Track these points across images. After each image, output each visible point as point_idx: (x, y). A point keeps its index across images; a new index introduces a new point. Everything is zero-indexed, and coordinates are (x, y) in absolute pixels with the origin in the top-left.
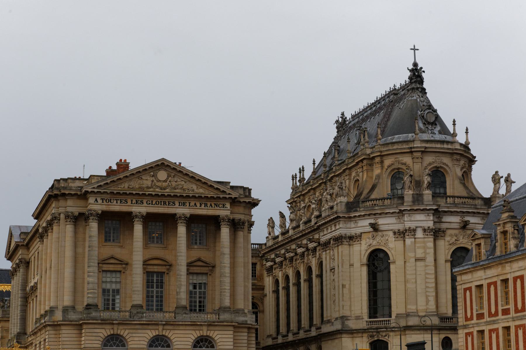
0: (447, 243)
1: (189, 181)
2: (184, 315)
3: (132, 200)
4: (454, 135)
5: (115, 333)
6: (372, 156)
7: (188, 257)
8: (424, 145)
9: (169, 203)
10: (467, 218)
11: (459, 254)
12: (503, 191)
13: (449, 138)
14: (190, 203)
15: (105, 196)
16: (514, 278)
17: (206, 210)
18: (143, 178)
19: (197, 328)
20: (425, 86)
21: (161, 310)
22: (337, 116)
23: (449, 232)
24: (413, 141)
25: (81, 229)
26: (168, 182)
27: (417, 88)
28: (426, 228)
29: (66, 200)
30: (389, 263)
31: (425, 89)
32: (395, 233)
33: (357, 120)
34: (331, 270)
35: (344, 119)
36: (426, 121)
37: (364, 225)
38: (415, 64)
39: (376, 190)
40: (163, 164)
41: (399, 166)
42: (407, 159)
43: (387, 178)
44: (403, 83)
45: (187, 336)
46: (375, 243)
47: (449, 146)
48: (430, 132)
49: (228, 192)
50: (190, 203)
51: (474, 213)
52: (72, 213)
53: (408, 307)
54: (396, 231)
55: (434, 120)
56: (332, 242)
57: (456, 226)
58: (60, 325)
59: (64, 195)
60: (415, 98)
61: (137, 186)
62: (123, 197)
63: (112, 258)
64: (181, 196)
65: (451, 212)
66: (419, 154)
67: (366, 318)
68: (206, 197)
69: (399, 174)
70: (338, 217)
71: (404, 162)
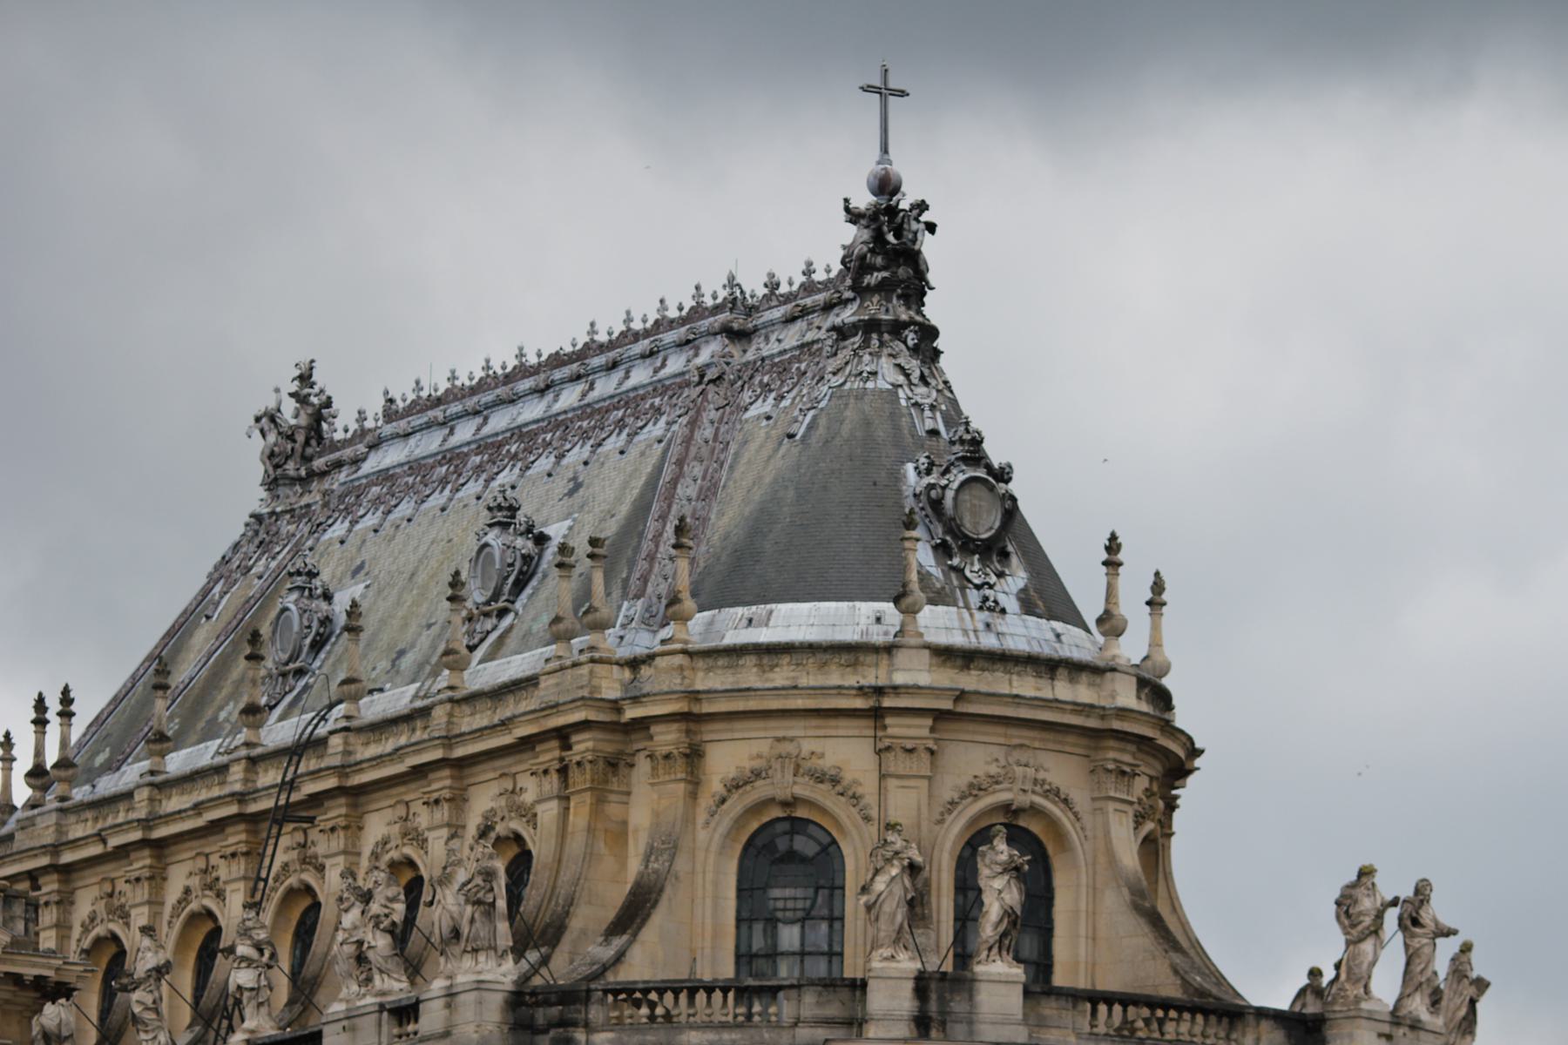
4: (1110, 624)
6: (631, 713)
8: (948, 678)
12: (1385, 985)
13: (1078, 644)
20: (934, 309)
22: (271, 387)
24: (889, 649)
27: (897, 328)
33: (431, 443)
35: (319, 414)
36: (952, 527)
38: (886, 186)
39: (658, 919)
41: (799, 791)
42: (848, 752)
43: (723, 850)
44: (791, 276)
47: (1083, 693)
55: (983, 528)
60: (882, 384)
66: (919, 729)
69: (792, 833)
71: (827, 763)
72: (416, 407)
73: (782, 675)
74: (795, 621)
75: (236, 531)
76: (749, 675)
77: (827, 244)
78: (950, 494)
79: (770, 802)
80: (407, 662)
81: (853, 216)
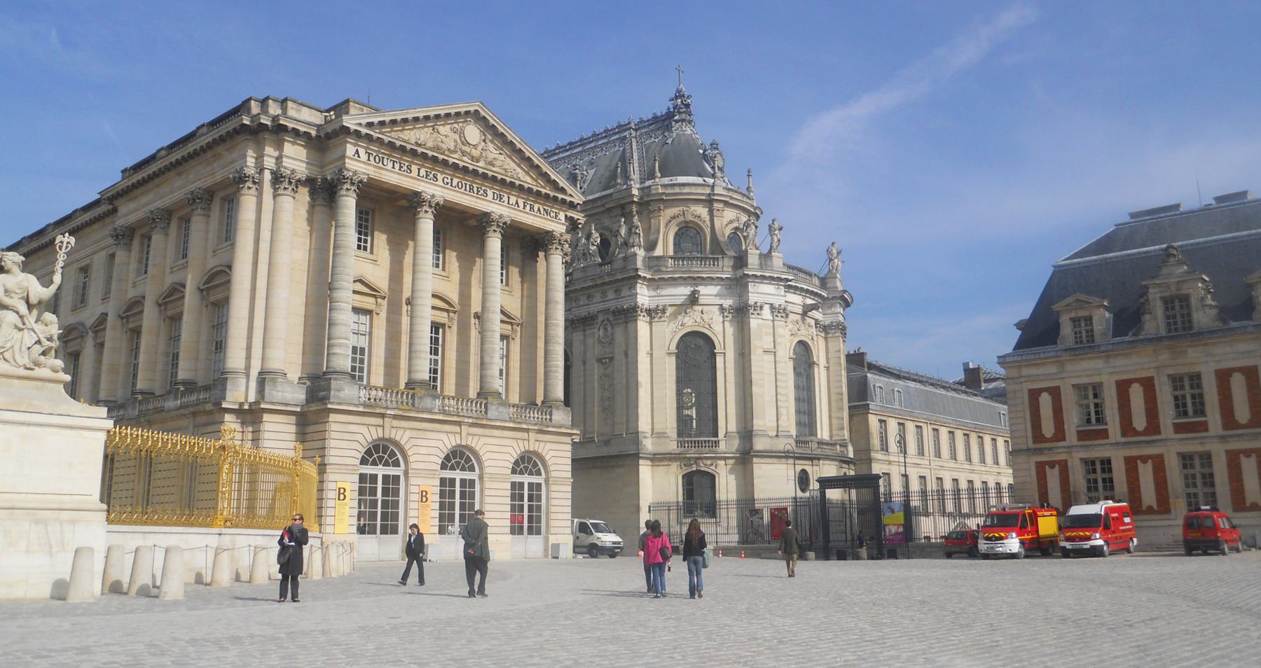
2: (501, 409)
5: (387, 436)
16: (1217, 372)
18: (441, 129)
19: (519, 435)
26: (480, 148)
34: (599, 360)
42: (702, 211)
45: (504, 450)
49: (569, 192)
53: (755, 421)
56: (601, 318)
61: (430, 144)
63: (360, 281)
64: (503, 182)
66: (720, 206)
67: (673, 433)
68: (538, 193)
73: (687, 190)
77: (661, 107)
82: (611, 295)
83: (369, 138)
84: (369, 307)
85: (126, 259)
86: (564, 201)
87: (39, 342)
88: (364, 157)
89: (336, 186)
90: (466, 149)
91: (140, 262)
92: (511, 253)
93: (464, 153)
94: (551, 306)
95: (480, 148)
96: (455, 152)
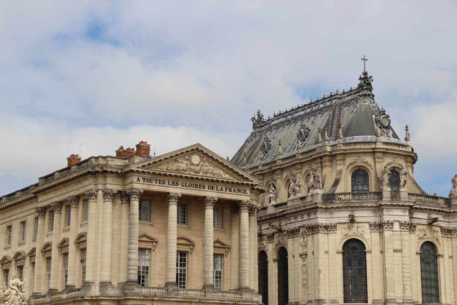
0: (418, 237)
1: (217, 166)
2: (213, 294)
3: (169, 181)
6: (333, 153)
7: (214, 238)
9: (200, 187)
10: (434, 216)
11: (425, 247)
14: (217, 187)
15: (147, 176)
17: (231, 195)
18: (179, 161)
20: (373, 92)
21: (184, 287)
23: (418, 227)
24: (375, 143)
25: (117, 207)
26: (200, 166)
27: (369, 95)
28: (403, 222)
29: (105, 177)
30: (366, 252)
31: (373, 96)
32: (371, 225)
34: (301, 256)
36: (382, 125)
37: (344, 216)
40: (197, 148)
41: (362, 164)
42: (369, 159)
46: (351, 233)
47: (404, 149)
48: (386, 135)
49: (250, 179)
50: (217, 187)
51: (439, 211)
52: (111, 190)
53: (388, 294)
54: (373, 223)
56: (302, 230)
57: (425, 222)
58: (96, 300)
59: (105, 172)
62: (162, 178)
63: (145, 236)
64: (212, 180)
65: (421, 209)
66: (380, 155)
68: (233, 183)
70: (318, 207)
72: (280, 114)
73: (358, 147)
74: (357, 138)
75: (249, 134)
76: (353, 147)
78: (381, 119)
79: (357, 166)
80: (287, 150)
81: (361, 79)
82: (306, 217)
83: (143, 172)
84: (149, 247)
85: (43, 223)
86: (248, 184)
87: (21, 298)
88: (142, 181)
89: (130, 196)
90: (193, 167)
91: (49, 224)
92: (224, 211)
93: (191, 170)
94: (242, 239)
95: (200, 165)
96: (187, 170)
